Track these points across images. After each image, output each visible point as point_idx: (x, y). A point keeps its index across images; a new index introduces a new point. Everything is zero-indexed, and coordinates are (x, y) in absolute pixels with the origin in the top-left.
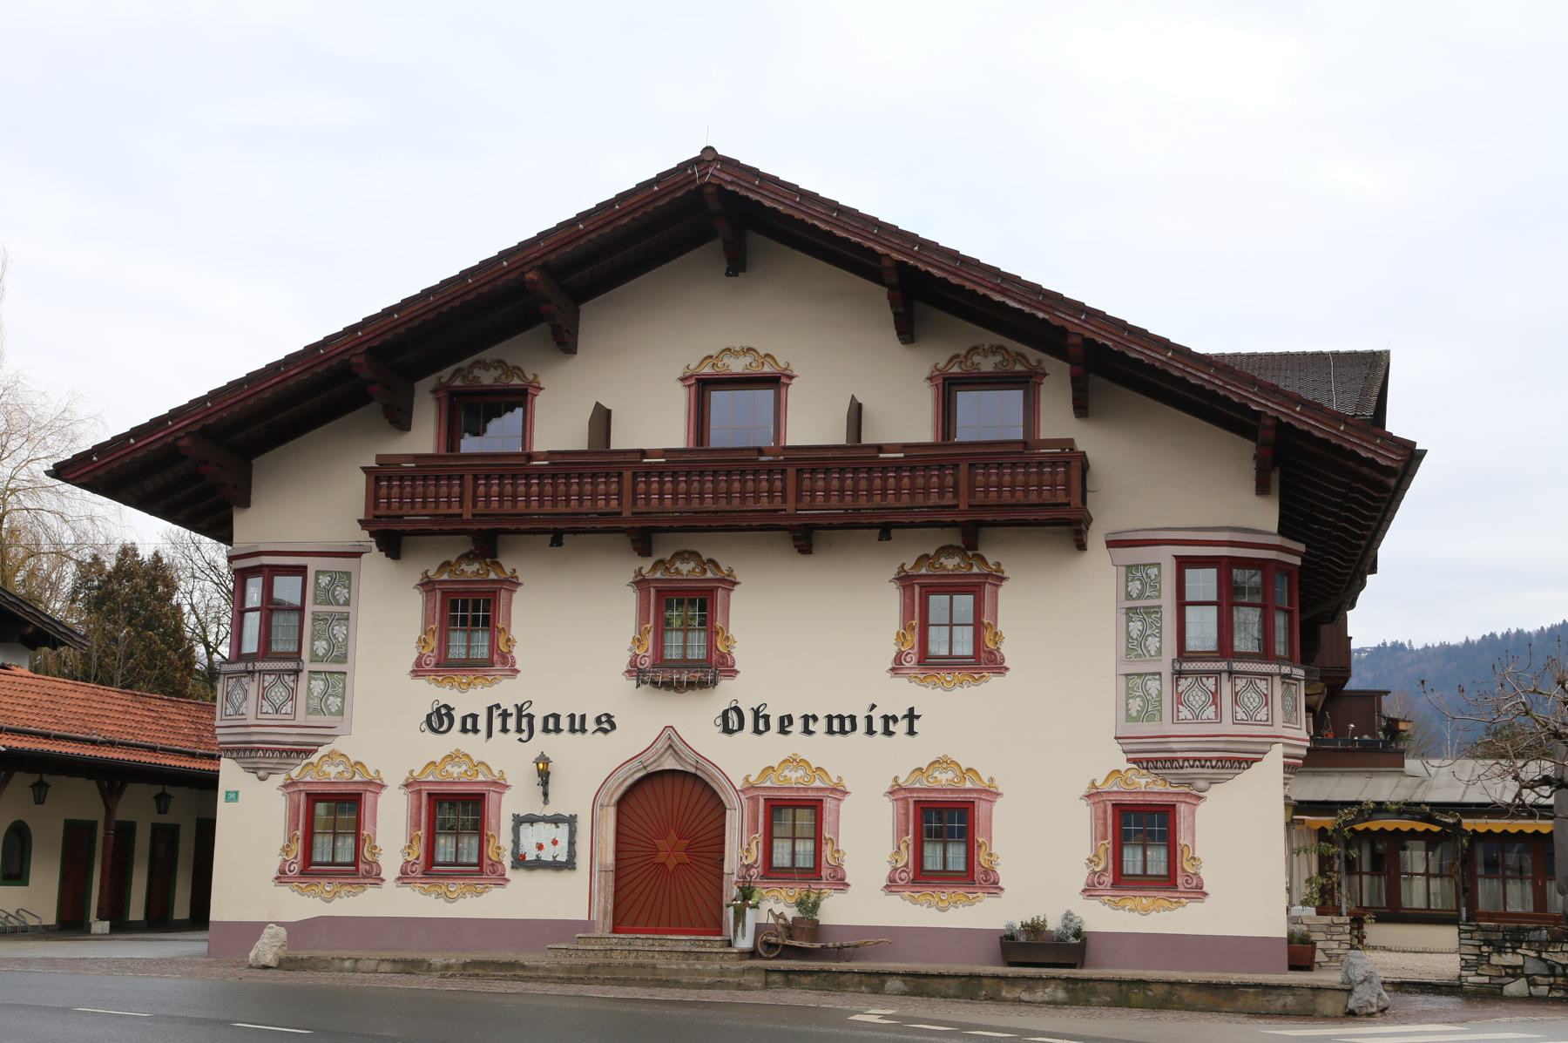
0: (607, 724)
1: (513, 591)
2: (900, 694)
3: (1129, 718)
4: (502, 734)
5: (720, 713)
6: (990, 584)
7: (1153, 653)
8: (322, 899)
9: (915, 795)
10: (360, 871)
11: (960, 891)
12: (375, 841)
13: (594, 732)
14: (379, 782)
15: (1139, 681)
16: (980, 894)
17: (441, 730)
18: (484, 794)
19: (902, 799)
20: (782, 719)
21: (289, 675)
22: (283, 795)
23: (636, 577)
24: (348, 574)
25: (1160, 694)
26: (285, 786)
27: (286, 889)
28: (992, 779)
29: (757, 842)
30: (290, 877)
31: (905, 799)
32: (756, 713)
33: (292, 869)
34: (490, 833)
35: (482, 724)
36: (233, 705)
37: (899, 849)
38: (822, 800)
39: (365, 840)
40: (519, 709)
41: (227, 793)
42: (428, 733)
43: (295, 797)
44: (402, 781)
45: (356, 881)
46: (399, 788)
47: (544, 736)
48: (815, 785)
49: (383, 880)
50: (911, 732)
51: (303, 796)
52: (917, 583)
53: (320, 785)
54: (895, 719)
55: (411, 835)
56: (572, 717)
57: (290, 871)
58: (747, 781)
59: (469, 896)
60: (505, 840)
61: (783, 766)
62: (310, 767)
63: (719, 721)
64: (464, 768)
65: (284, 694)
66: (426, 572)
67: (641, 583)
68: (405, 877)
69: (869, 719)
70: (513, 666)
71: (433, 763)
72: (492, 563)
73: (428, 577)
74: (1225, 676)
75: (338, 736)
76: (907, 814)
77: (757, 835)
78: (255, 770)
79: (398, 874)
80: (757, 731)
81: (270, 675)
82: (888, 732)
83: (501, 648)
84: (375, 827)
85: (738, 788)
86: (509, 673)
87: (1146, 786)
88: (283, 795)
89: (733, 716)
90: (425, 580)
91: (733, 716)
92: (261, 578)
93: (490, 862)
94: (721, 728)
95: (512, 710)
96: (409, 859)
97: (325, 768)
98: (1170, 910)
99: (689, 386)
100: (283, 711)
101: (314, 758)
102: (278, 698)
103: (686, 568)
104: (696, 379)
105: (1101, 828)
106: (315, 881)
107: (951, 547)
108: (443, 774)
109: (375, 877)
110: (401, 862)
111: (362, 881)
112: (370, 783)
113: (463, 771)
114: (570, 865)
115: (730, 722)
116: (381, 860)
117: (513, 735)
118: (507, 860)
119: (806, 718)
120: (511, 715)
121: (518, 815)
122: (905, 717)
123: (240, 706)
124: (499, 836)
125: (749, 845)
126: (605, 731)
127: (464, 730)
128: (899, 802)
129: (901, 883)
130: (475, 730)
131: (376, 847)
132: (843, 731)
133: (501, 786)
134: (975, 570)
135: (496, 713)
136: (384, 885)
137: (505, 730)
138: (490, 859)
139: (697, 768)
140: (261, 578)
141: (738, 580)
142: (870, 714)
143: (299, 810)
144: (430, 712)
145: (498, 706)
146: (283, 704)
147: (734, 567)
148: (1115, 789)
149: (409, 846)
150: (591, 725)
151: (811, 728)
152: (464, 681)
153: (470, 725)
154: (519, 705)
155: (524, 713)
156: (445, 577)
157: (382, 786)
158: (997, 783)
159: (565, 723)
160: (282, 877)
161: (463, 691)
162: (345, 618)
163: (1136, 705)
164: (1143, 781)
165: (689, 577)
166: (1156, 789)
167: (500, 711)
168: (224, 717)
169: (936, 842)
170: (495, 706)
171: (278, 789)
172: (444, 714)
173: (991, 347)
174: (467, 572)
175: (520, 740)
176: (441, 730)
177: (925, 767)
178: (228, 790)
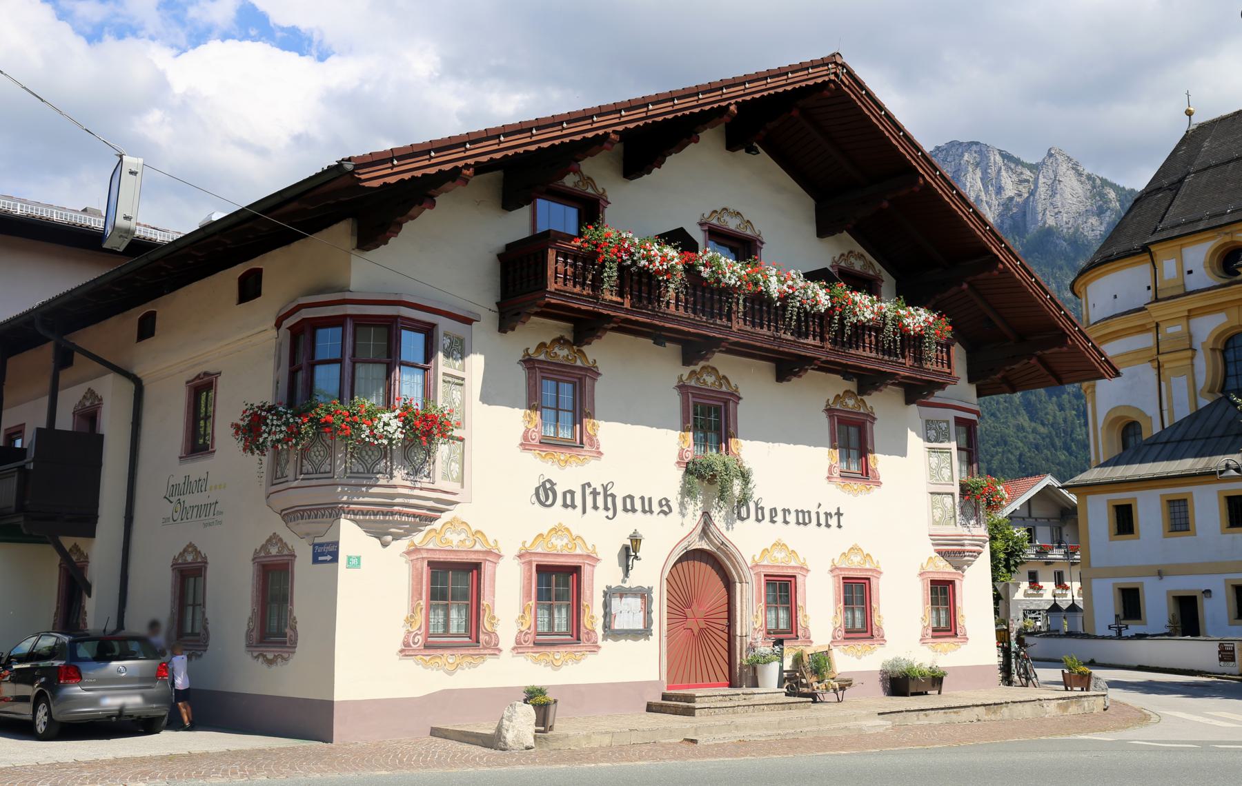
1: (595, 380)
3: (935, 522)
6: (869, 421)
9: (843, 573)
10: (481, 641)
12: (493, 610)
13: (658, 514)
14: (496, 551)
16: (876, 645)
17: (548, 503)
18: (581, 566)
19: (837, 576)
23: (679, 382)
26: (408, 553)
27: (410, 662)
28: (878, 562)
29: (762, 610)
31: (838, 576)
35: (578, 501)
36: (312, 462)
37: (836, 613)
38: (794, 577)
39: (484, 610)
40: (605, 489)
41: (349, 558)
42: (537, 504)
44: (516, 552)
45: (477, 652)
47: (624, 514)
49: (500, 650)
50: (839, 526)
52: (837, 415)
53: (442, 552)
54: (830, 514)
55: (524, 605)
56: (642, 498)
57: (414, 643)
58: (754, 560)
60: (598, 611)
61: (773, 548)
62: (433, 534)
64: (565, 541)
66: (527, 349)
67: (682, 388)
69: (818, 513)
70: (598, 448)
71: (541, 535)
72: (578, 350)
73: (528, 355)
75: (459, 503)
76: (839, 587)
77: (761, 604)
78: (378, 535)
79: (513, 644)
80: (758, 520)
82: (828, 526)
83: (589, 431)
84: (494, 597)
85: (749, 566)
86: (596, 455)
87: (943, 569)
88: (406, 562)
90: (527, 357)
92: (403, 332)
95: (600, 489)
96: (522, 629)
97: (448, 535)
98: (955, 650)
99: (705, 231)
101: (437, 525)
102: (370, 457)
103: (710, 380)
105: (926, 597)
108: (550, 546)
109: (495, 650)
110: (515, 632)
111: (483, 652)
112: (489, 552)
113: (564, 545)
114: (645, 633)
116: (500, 630)
117: (602, 513)
118: (599, 631)
119: (784, 510)
120: (599, 493)
121: (611, 587)
122: (836, 514)
123: (322, 463)
124: (592, 606)
126: (665, 513)
127: (565, 505)
128: (836, 578)
130: (574, 506)
131: (494, 617)
132: (805, 524)
133: (593, 559)
134: (862, 411)
135: (588, 491)
136: (502, 655)
137: (595, 507)
138: (586, 628)
139: (718, 548)
140: (403, 332)
141: (741, 396)
142: (819, 510)
143: (422, 578)
144: (538, 485)
145: (589, 485)
148: (931, 570)
149: (522, 616)
150: (656, 508)
154: (605, 486)
155: (609, 493)
156: (542, 357)
157: (499, 556)
158: (880, 565)
160: (406, 650)
161: (562, 468)
163: (938, 513)
165: (712, 388)
167: (591, 490)
170: (587, 484)
171: (401, 556)
172: (549, 489)
174: (559, 355)
175: (607, 517)
176: (548, 503)
177: (847, 552)
178: (350, 555)
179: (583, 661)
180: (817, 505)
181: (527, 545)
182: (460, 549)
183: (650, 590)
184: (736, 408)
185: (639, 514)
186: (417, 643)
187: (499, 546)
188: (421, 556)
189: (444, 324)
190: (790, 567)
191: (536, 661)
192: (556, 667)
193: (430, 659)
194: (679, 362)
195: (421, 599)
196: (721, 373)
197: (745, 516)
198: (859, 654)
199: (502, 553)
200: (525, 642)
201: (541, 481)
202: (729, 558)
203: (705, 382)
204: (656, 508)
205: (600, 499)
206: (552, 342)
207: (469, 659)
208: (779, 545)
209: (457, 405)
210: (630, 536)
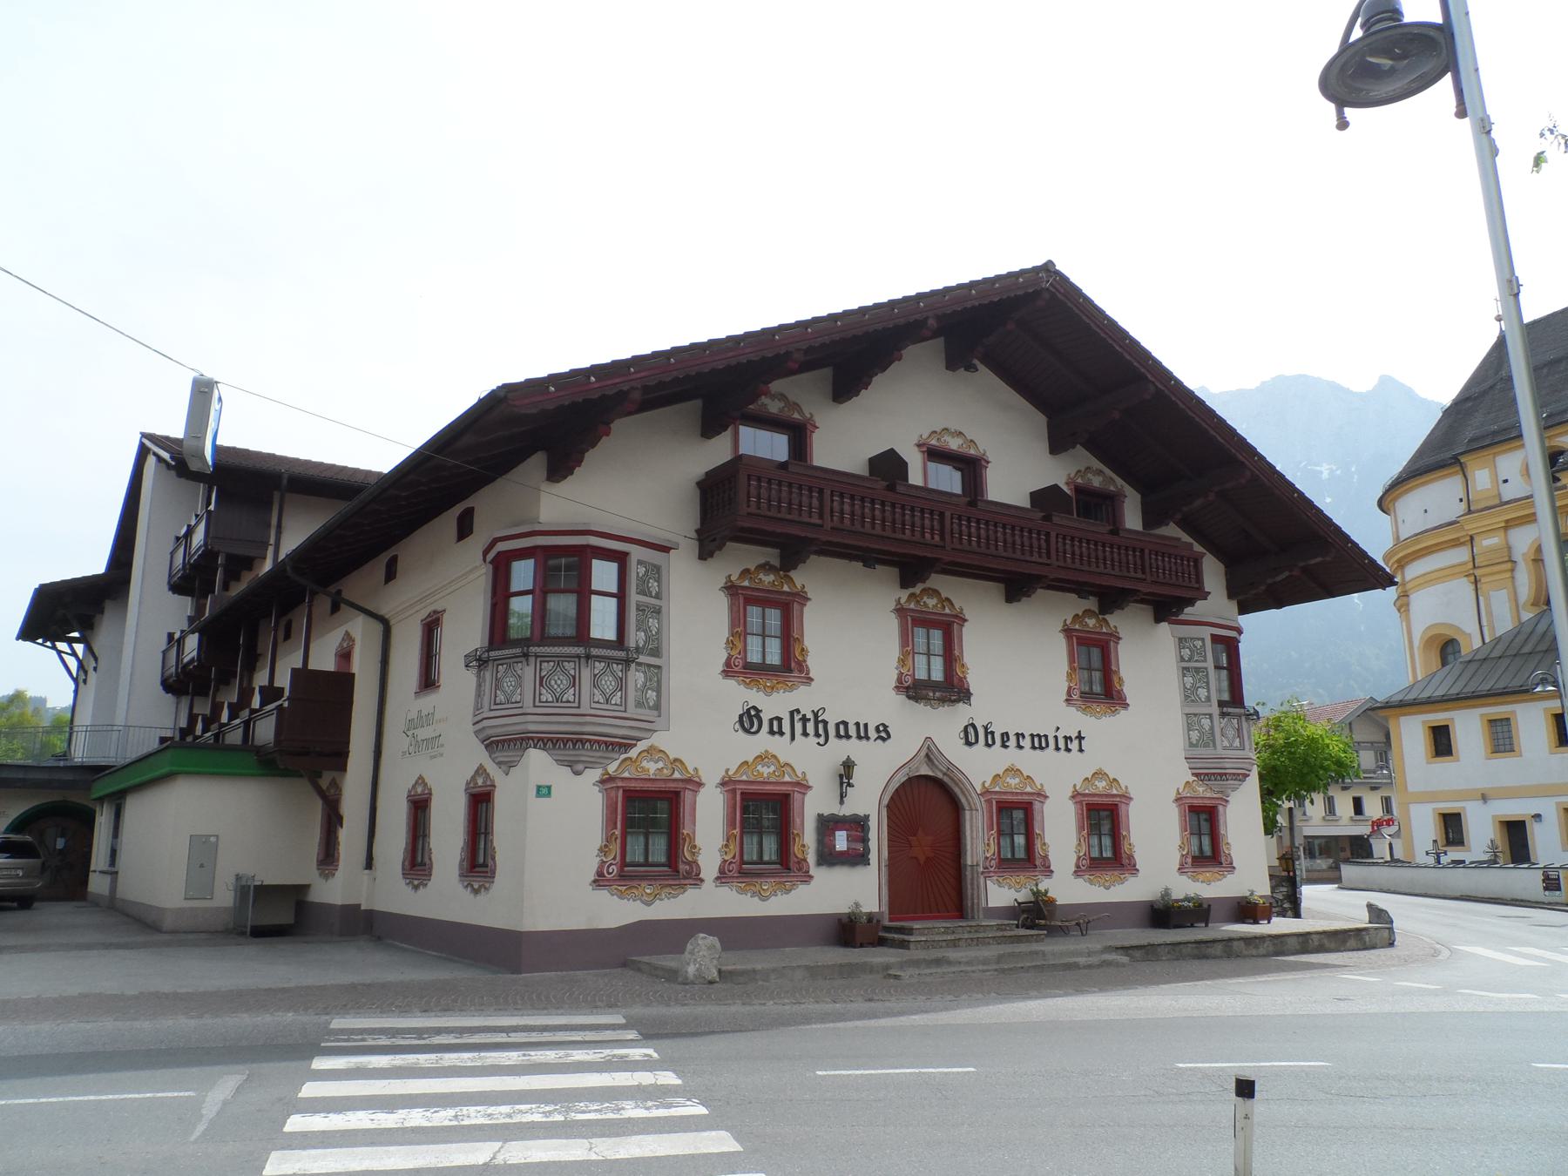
0: (884, 733)
2: (1073, 720)
3: (1191, 745)
4: (803, 738)
5: (962, 728)
7: (1203, 700)
8: (643, 902)
10: (681, 871)
11: (1116, 873)
13: (875, 740)
15: (1195, 719)
17: (752, 730)
20: (1002, 735)
21: (618, 664)
22: (599, 791)
24: (658, 569)
25: (1212, 728)
26: (602, 782)
28: (1126, 787)
30: (608, 880)
31: (1081, 802)
32: (986, 728)
33: (611, 871)
34: (795, 832)
35: (786, 728)
39: (685, 840)
40: (816, 715)
42: (740, 732)
43: (613, 794)
46: (716, 787)
47: (836, 740)
48: (1026, 790)
49: (702, 880)
50: (1081, 750)
51: (621, 792)
53: (639, 781)
54: (1070, 738)
56: (857, 724)
57: (609, 874)
59: (780, 893)
62: (628, 762)
63: (962, 735)
64: (772, 768)
65: (613, 683)
66: (730, 576)
67: (900, 611)
68: (723, 877)
69: (1056, 737)
70: (808, 674)
71: (746, 763)
72: (785, 576)
73: (731, 581)
74: (1243, 718)
76: (1083, 814)
78: (570, 764)
79: (715, 873)
80: (988, 745)
81: (600, 662)
82: (1068, 750)
84: (695, 825)
85: (979, 792)
87: (1202, 792)
88: (599, 791)
89: (971, 730)
90: (729, 584)
91: (971, 730)
93: (796, 860)
94: (963, 741)
95: (810, 716)
96: (726, 858)
98: (1219, 880)
99: (923, 452)
100: (613, 702)
101: (633, 753)
103: (932, 602)
104: (928, 448)
105: (1184, 823)
106: (635, 883)
107: (1089, 610)
109: (695, 878)
110: (718, 862)
111: (683, 882)
115: (970, 735)
116: (701, 860)
117: (812, 740)
118: (811, 858)
119: (1017, 735)
122: (1076, 738)
123: (513, 692)
125: (989, 840)
126: (884, 739)
127: (772, 732)
129: (1083, 868)
130: (781, 733)
131: (695, 847)
132: (1041, 748)
133: (803, 786)
134: (1104, 630)
135: (797, 717)
136: (704, 886)
137: (805, 734)
138: (797, 857)
139: (945, 774)
141: (967, 617)
144: (742, 712)
145: (798, 711)
146: (613, 694)
147: (964, 608)
148: (1188, 795)
149: (726, 845)
150: (872, 734)
151: (1069, 746)
152: (768, 684)
153: (776, 728)
155: (820, 719)
156: (746, 583)
158: (1130, 790)
159: (852, 731)
160: (600, 881)
162: (657, 611)
163: (1195, 735)
164: (1201, 789)
166: (1208, 795)
167: (800, 716)
168: (537, 704)
169: (753, 832)
171: (594, 784)
173: (1097, 470)
175: (818, 744)
176: (752, 730)
177: (1090, 777)
178: (539, 784)
179: (793, 891)
180: (1055, 729)
181: (730, 773)
182: (658, 777)
183: (867, 817)
184: (961, 631)
185: (854, 740)
186: (611, 873)
187: (700, 773)
188: (615, 785)
189: (636, 553)
190: (1025, 793)
191: (742, 891)
192: (764, 899)
193: (627, 889)
194: (898, 585)
195: (616, 828)
196: (944, 595)
197: (973, 741)
198: (1107, 884)
199: (704, 781)
200: (730, 871)
201: (746, 708)
202: (957, 784)
203: (925, 605)
204: (872, 734)
205: (810, 727)
206: (757, 567)
207: (668, 890)
208: (1013, 771)
209: (654, 633)
210: (844, 762)
